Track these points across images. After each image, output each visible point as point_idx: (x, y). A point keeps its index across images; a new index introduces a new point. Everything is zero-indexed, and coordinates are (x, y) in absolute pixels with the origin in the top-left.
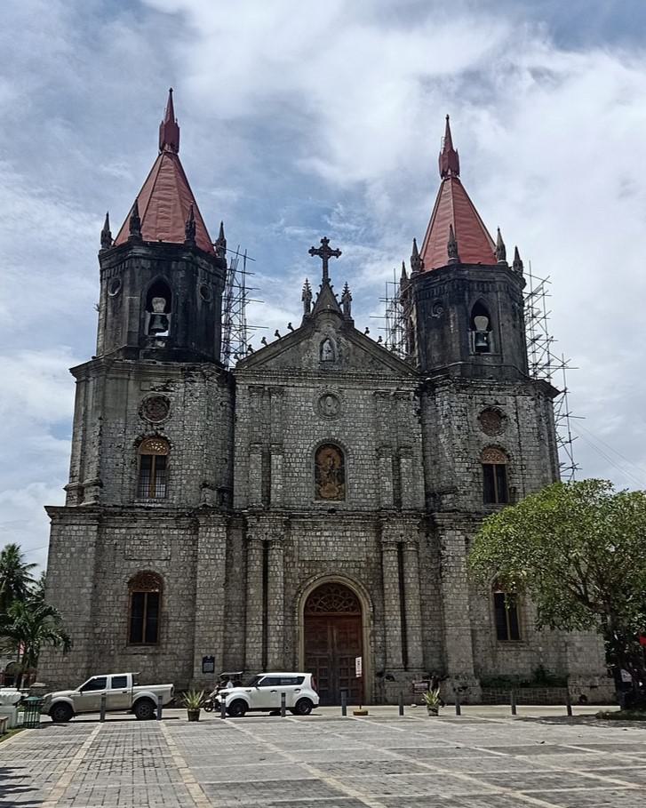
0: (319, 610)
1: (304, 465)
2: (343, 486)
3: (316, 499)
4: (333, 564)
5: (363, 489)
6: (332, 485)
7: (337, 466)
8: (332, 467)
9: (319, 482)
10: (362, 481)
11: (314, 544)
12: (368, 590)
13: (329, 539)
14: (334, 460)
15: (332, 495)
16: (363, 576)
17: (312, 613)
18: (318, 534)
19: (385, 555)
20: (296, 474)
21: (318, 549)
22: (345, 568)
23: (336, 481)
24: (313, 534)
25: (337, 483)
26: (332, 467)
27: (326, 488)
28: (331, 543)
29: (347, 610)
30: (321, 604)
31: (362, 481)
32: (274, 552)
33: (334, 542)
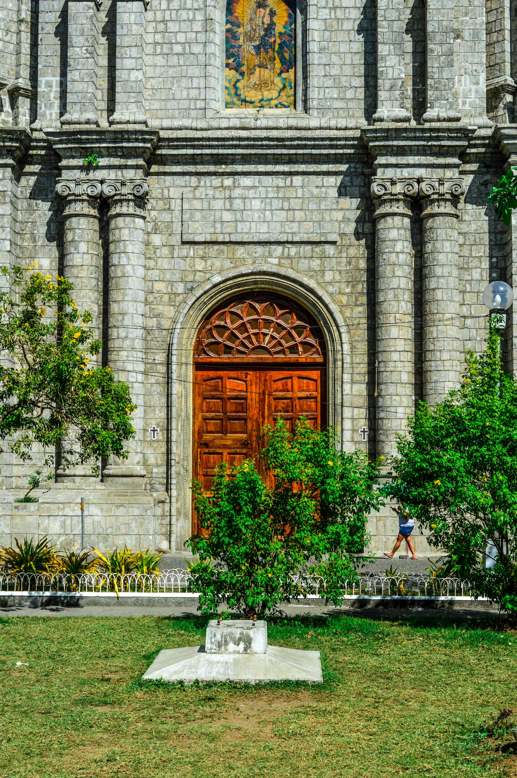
0: (228, 349)
1: (198, 26)
2: (292, 71)
3: (228, 105)
4: (259, 250)
5: (334, 77)
6: (266, 73)
7: (279, 28)
8: (270, 29)
9: (237, 68)
10: (335, 59)
11: (218, 204)
12: (342, 306)
13: (251, 193)
14: (272, 13)
15: (267, 95)
16: (329, 276)
17: (213, 357)
18: (228, 181)
19: (381, 225)
20: (178, 49)
21: (227, 216)
22: (289, 257)
23: (277, 61)
24: (216, 181)
25: (278, 65)
26: (271, 26)
27: (255, 79)
28: (257, 204)
29: (293, 349)
30: (243, 344)
31: (335, 59)
32: (120, 222)
33: (263, 200)
